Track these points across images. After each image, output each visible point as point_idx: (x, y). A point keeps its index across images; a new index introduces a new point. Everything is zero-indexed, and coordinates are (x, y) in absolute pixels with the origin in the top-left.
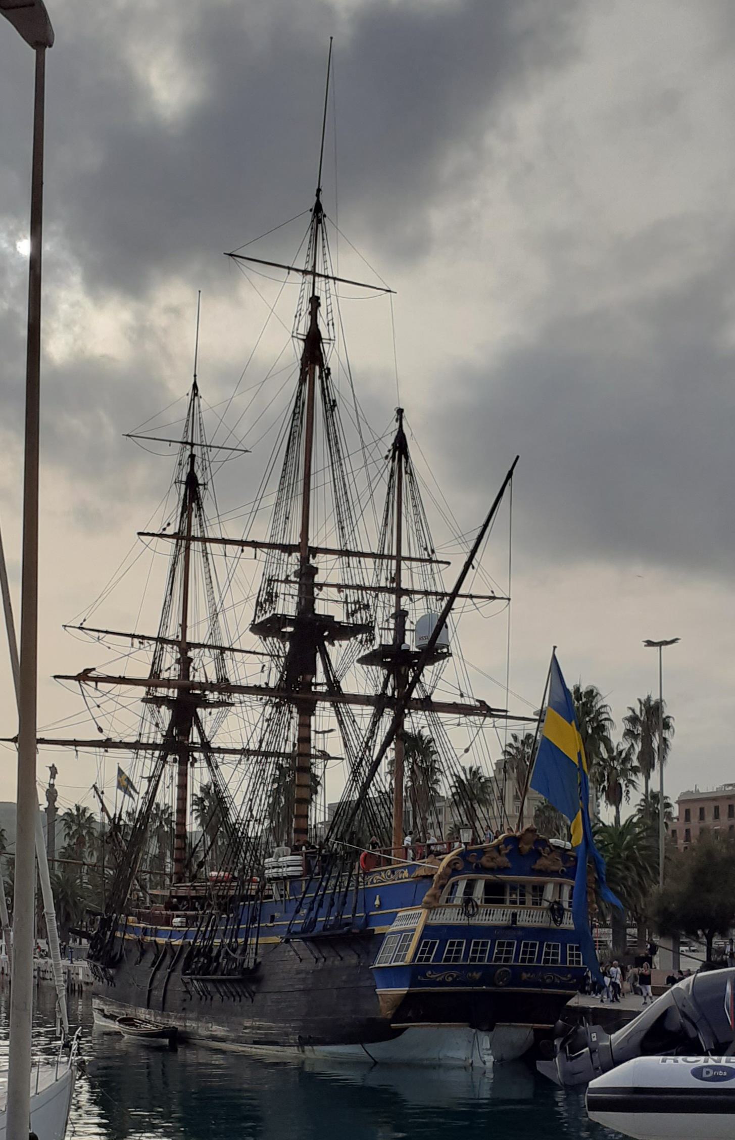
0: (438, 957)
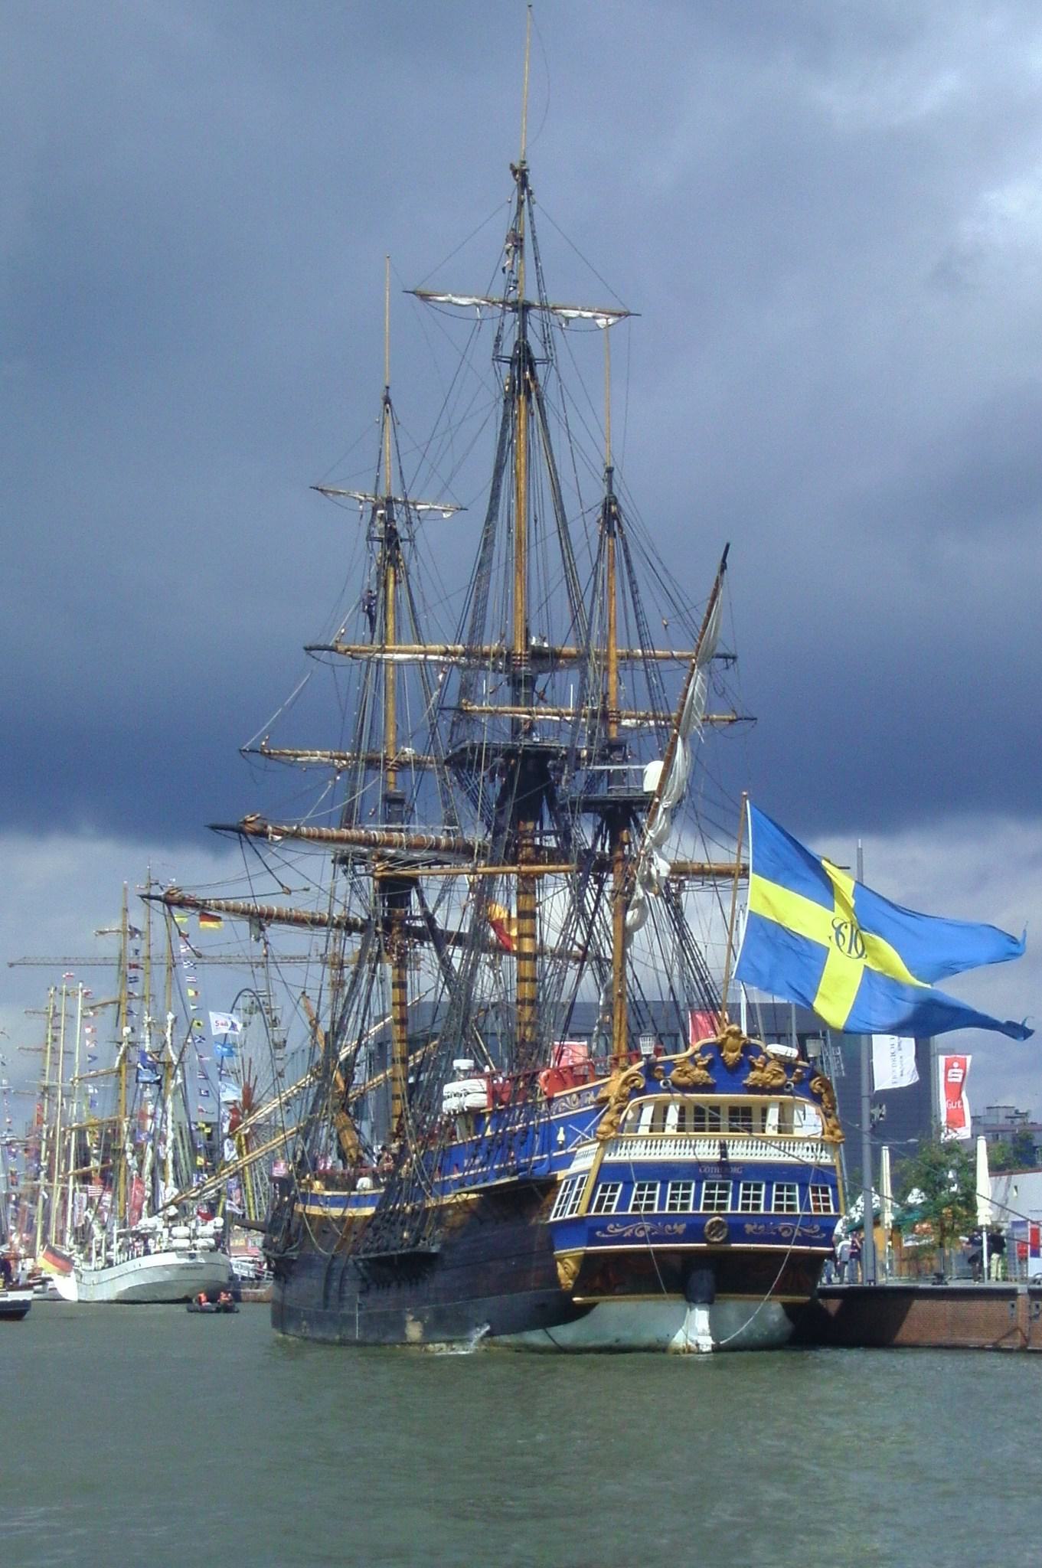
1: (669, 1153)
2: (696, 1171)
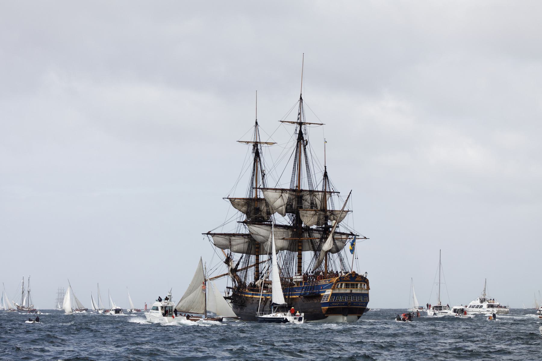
0: (335, 300)
1: (342, 291)
2: (346, 294)
